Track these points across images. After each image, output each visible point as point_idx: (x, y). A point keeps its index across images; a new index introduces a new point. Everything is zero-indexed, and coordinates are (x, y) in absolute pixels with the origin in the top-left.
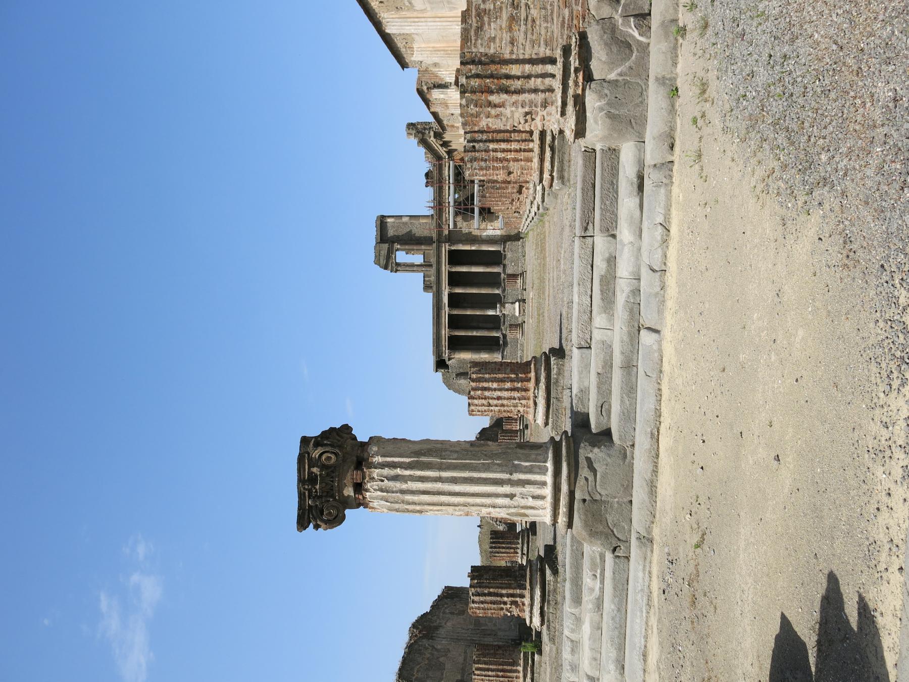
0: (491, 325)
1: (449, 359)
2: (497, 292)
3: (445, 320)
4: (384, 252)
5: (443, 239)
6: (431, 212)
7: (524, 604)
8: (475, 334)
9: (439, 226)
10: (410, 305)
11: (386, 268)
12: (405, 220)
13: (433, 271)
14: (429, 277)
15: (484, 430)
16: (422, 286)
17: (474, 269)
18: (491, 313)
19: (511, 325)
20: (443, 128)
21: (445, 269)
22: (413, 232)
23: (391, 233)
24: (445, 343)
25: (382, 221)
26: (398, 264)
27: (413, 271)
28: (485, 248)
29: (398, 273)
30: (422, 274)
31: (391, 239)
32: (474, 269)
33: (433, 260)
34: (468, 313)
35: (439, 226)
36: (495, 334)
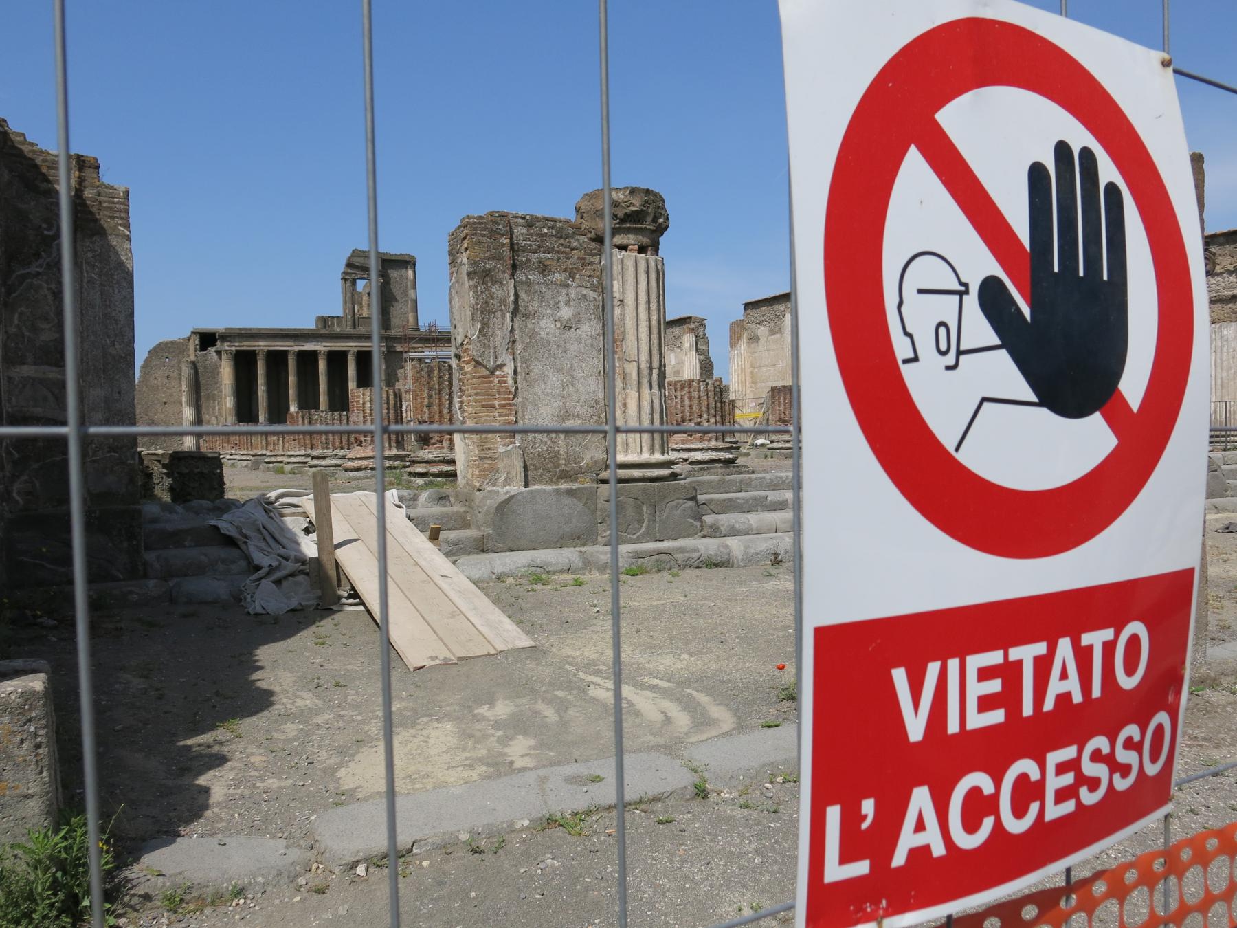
1: (219, 353)
3: (280, 346)
5: (390, 344)
6: (422, 329)
7: (709, 441)
9: (408, 339)
10: (297, 297)
11: (349, 265)
12: (412, 292)
13: (347, 329)
21: (352, 346)
22: (395, 304)
23: (394, 274)
24: (246, 345)
25: (407, 262)
26: (354, 282)
27: (345, 302)
29: (340, 283)
30: (341, 314)
35: (408, 339)
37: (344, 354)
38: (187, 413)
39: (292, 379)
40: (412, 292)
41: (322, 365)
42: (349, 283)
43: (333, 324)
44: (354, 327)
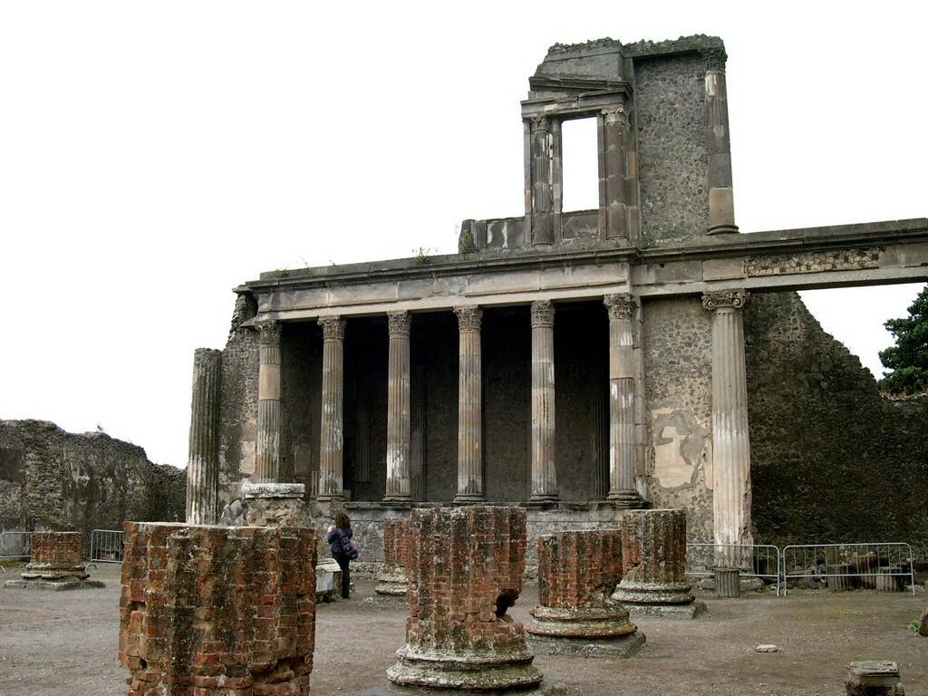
2: (462, 483)
4: (589, 71)
8: (326, 408)
11: (538, 83)
14: (512, 237)
15: (140, 452)
16: (480, 216)
17: (542, 395)
28: (617, 430)
29: (520, 127)
30: (518, 210)
31: (651, 93)
32: (542, 395)
33: (568, 245)
34: (391, 383)
37: (521, 313)
39: (398, 384)
41: (469, 345)
43: (498, 238)
44: (551, 239)
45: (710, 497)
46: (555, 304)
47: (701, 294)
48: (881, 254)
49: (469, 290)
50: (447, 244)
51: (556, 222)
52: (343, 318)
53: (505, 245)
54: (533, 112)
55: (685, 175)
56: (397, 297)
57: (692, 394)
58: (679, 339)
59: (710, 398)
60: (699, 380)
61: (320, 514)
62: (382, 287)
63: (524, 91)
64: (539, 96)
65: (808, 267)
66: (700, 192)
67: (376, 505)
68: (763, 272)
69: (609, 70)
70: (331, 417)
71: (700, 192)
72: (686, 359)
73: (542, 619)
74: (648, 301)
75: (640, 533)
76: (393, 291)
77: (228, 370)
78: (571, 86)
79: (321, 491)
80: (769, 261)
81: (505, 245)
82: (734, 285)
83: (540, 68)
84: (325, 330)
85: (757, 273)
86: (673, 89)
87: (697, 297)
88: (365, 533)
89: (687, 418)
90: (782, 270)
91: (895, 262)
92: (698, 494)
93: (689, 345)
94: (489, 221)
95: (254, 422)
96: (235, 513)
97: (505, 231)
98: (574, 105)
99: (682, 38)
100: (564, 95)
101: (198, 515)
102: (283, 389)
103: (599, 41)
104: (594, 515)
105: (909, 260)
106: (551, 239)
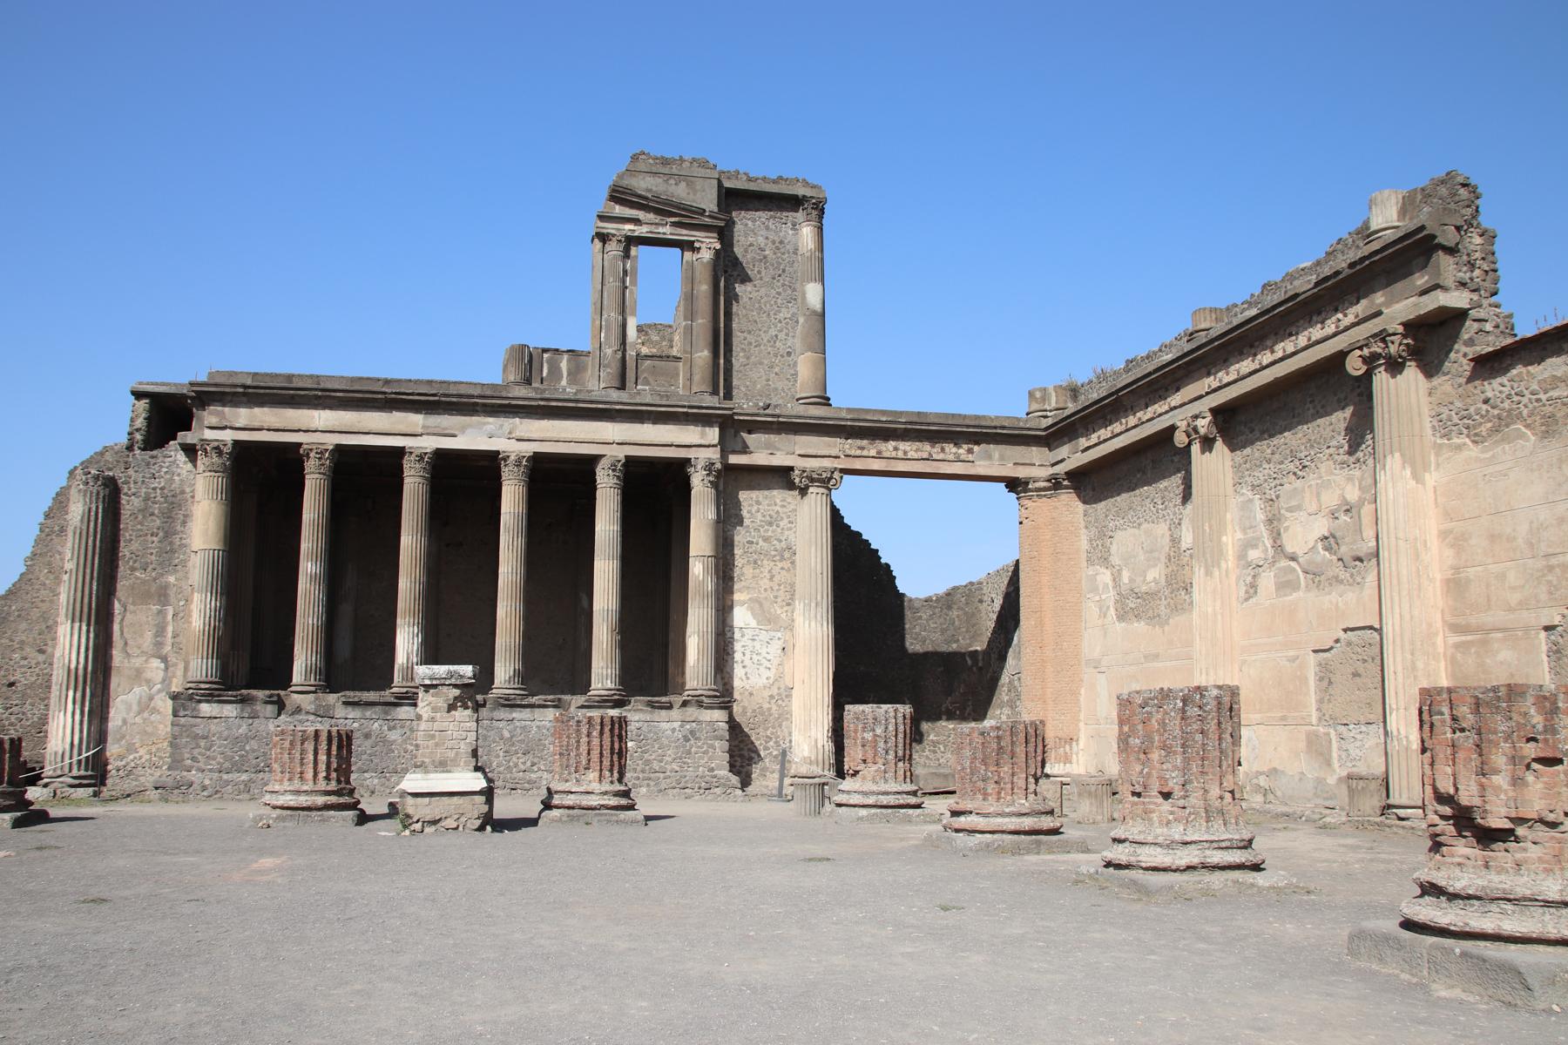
0: (344, 649)
1: (190, 451)
3: (374, 429)
8: (309, 568)
11: (619, 195)
12: (813, 293)
14: (576, 373)
16: (535, 342)
18: (406, 641)
19: (344, 742)
20: (1489, 365)
30: (584, 344)
33: (643, 393)
36: (304, 660)
38: (69, 644)
39: (411, 542)
40: (813, 293)
41: (512, 499)
42: (614, 248)
43: (555, 370)
44: (622, 387)
45: (789, 696)
46: (630, 461)
47: (791, 469)
48: (976, 448)
49: (517, 434)
50: (486, 369)
51: (631, 364)
52: (339, 448)
53: (564, 382)
54: (610, 228)
55: (773, 332)
56: (420, 431)
57: (771, 579)
58: (759, 516)
59: (792, 585)
60: (780, 565)
61: (298, 710)
62: (397, 415)
63: (601, 203)
64: (619, 210)
65: (905, 453)
66: (789, 354)
67: (387, 695)
68: (858, 452)
69: (707, 200)
70: (313, 578)
71: (789, 354)
72: (766, 540)
73: (986, 815)
74: (729, 469)
75: (879, 731)
76: (416, 420)
77: (130, 504)
78: (663, 208)
79: (297, 677)
80: (865, 442)
81: (564, 382)
82: (827, 463)
83: (621, 176)
84: (311, 465)
85: (853, 453)
86: (763, 232)
87: (787, 471)
88: (367, 736)
89: (766, 605)
90: (879, 452)
91: (990, 457)
92: (775, 691)
93: (770, 524)
94: (545, 351)
95: (172, 579)
96: (135, 708)
97: (564, 365)
98: (661, 230)
99: (781, 178)
100: (651, 216)
101: (78, 712)
102: (430, 537)
103: (694, 160)
104: (675, 713)
105: (1002, 458)
106: (622, 387)
